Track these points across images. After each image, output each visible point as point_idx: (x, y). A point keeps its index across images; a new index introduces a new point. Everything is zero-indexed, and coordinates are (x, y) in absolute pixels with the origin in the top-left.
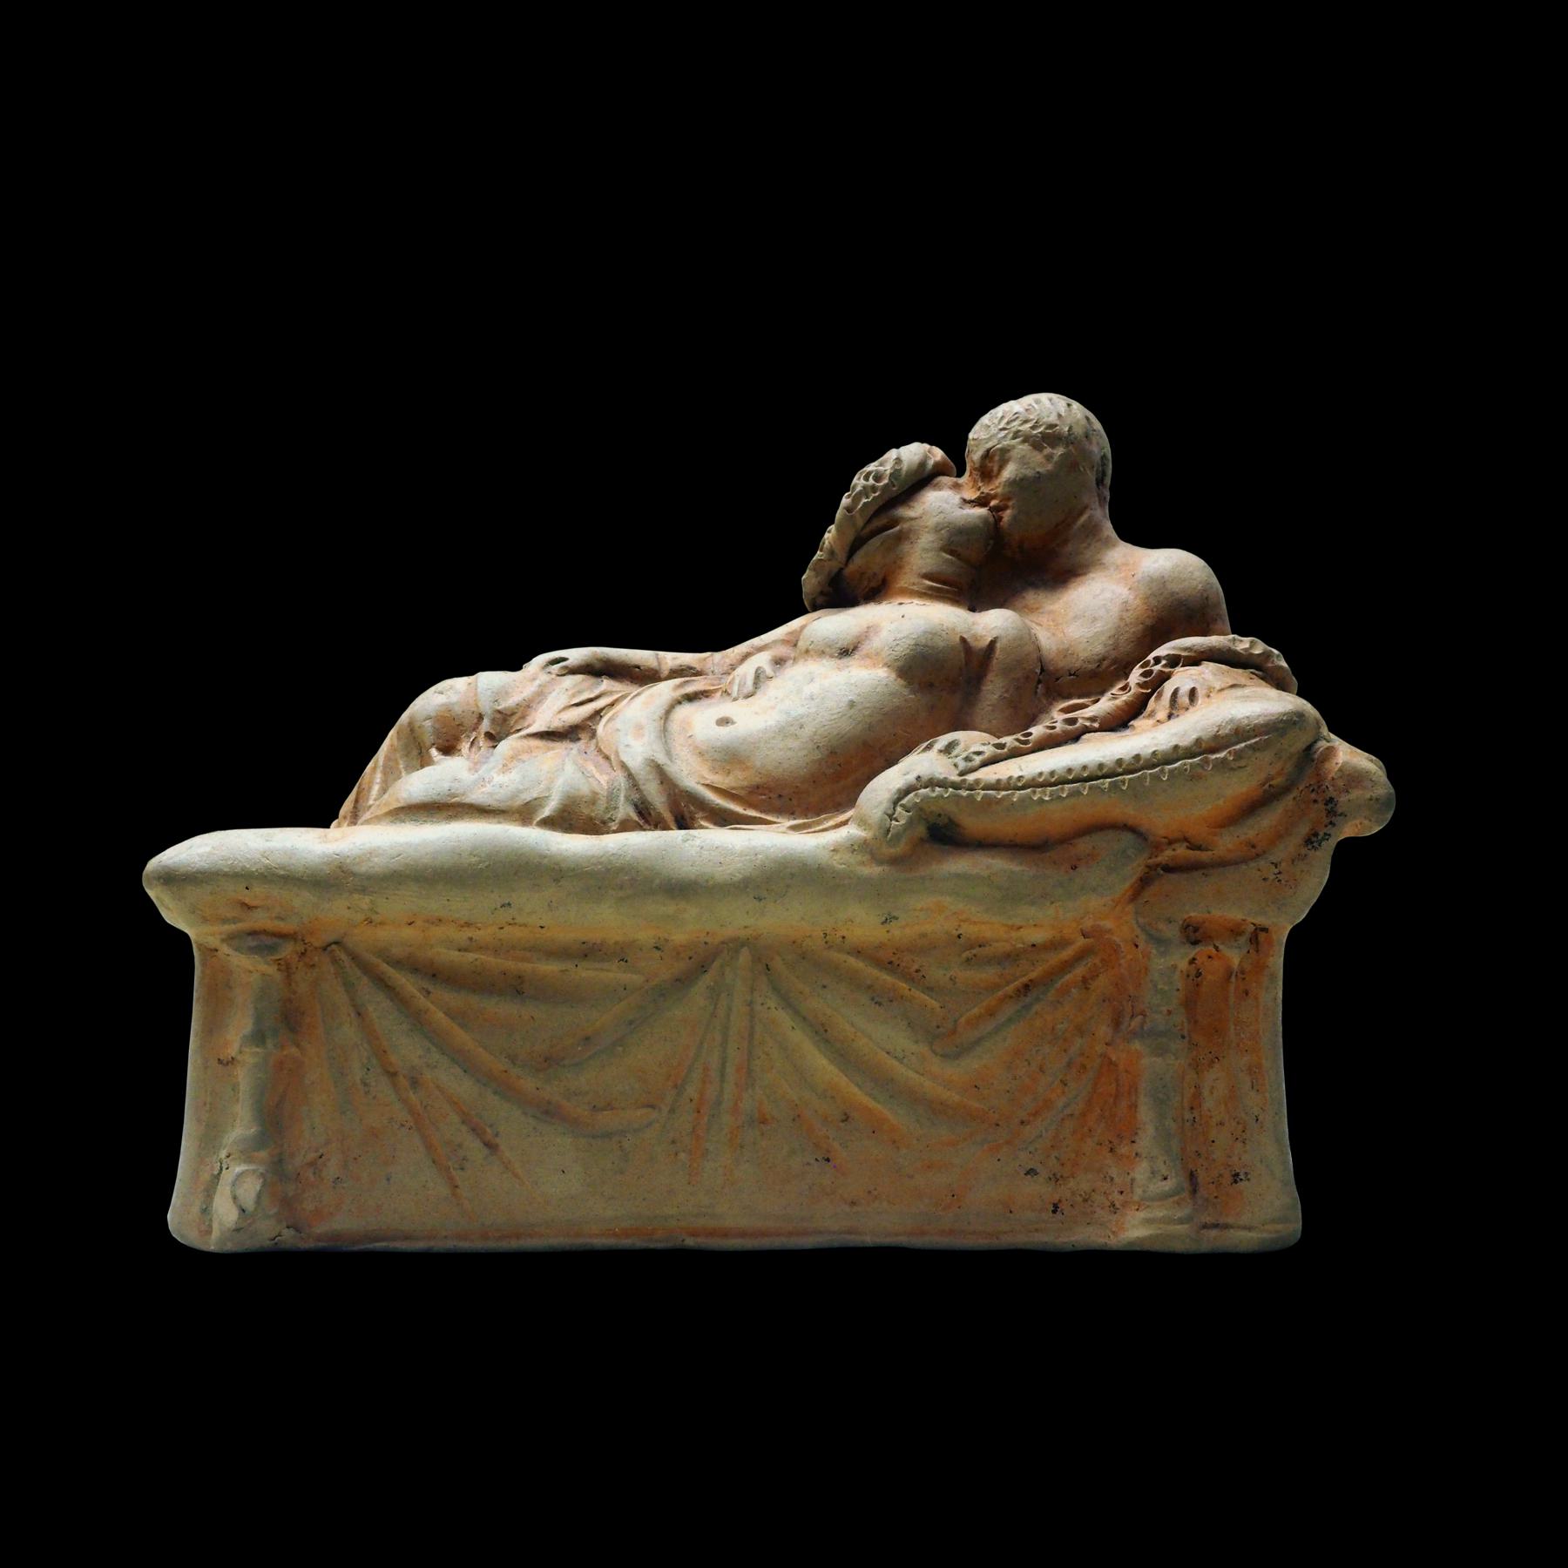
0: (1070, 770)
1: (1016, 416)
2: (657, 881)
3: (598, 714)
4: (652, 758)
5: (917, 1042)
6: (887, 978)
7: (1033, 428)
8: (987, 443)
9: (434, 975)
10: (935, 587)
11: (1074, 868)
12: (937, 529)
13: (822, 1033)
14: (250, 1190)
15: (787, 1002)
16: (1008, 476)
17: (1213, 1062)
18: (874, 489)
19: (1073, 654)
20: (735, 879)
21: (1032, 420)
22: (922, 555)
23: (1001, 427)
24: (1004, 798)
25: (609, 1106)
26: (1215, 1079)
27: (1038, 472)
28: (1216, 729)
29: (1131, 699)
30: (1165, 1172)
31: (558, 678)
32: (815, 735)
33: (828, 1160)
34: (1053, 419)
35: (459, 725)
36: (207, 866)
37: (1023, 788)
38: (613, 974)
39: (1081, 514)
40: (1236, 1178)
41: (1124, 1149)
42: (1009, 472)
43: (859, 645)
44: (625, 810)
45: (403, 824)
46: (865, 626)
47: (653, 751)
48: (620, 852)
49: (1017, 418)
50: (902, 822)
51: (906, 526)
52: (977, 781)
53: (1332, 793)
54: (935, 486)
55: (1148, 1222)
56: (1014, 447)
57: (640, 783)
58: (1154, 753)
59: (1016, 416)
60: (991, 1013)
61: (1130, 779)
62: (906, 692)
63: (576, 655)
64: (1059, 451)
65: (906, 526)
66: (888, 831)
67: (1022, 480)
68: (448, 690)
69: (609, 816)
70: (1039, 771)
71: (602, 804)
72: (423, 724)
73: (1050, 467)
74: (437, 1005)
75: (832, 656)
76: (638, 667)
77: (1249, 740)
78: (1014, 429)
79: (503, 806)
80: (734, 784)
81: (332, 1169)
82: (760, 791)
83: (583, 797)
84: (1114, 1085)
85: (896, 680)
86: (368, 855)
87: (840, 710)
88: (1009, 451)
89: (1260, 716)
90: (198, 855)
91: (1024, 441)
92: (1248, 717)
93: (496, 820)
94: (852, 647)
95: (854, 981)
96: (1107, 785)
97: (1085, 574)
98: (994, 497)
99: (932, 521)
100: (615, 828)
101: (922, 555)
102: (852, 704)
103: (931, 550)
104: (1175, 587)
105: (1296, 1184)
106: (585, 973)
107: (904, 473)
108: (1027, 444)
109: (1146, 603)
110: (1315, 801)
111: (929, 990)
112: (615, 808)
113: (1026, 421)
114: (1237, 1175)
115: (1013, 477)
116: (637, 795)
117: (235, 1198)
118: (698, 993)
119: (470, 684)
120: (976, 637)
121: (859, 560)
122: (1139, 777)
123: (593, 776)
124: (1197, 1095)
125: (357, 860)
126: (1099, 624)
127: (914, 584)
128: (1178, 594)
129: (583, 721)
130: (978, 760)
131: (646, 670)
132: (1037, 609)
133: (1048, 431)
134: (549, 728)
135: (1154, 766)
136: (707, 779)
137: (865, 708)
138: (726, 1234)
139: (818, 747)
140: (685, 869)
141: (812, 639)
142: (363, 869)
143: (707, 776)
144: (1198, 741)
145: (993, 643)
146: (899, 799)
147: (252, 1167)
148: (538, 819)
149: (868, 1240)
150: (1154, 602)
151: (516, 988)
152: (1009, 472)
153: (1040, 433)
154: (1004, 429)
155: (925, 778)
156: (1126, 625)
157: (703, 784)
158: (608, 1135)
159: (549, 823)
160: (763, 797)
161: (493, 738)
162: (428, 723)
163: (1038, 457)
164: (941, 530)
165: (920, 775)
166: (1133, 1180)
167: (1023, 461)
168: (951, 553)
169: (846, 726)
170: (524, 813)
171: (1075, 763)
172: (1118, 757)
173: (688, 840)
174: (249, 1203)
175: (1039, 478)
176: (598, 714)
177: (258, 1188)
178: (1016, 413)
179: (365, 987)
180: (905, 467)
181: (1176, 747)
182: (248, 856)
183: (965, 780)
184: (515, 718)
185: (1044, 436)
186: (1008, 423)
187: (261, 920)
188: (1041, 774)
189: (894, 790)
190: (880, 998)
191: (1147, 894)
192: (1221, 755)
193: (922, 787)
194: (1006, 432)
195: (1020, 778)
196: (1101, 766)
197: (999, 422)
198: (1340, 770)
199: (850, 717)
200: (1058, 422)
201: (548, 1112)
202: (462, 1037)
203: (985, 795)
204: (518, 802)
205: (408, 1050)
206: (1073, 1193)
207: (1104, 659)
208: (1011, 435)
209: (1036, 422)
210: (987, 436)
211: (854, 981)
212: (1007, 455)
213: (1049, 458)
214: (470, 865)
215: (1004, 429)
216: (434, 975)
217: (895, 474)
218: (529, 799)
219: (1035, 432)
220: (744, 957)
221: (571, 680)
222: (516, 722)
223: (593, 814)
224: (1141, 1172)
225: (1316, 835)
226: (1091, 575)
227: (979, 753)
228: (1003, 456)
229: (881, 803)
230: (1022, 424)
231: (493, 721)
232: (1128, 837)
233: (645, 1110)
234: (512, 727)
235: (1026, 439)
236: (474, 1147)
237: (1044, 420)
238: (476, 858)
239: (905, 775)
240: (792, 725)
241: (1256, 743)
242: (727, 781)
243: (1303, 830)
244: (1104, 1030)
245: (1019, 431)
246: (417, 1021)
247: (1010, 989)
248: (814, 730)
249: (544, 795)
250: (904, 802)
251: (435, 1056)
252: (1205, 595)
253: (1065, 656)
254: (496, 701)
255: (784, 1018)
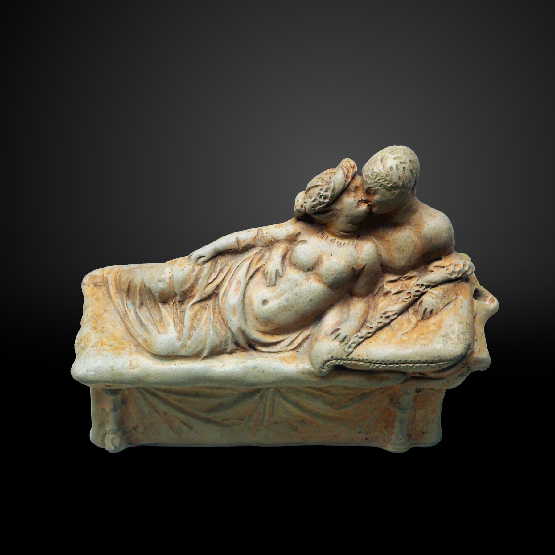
0: (383, 361)
1: (382, 177)
2: (244, 384)
3: (218, 287)
4: (240, 327)
5: (327, 406)
6: (319, 393)
7: (388, 184)
8: (369, 185)
9: (170, 392)
10: (346, 235)
11: (382, 380)
12: (347, 216)
13: (296, 405)
14: (117, 442)
15: (285, 398)
16: (376, 199)
17: (421, 409)
18: (323, 203)
19: (394, 263)
20: (270, 382)
21: (388, 180)
22: (341, 223)
23: (375, 181)
24: (360, 365)
25: (228, 419)
26: (420, 414)
27: (388, 199)
28: (433, 358)
29: (410, 302)
30: (401, 438)
31: (202, 266)
32: (297, 310)
33: (297, 430)
34: (396, 180)
35: (168, 296)
36: (94, 379)
37: (367, 362)
38: (228, 392)
39: (404, 205)
40: (423, 433)
41: (390, 429)
42: (376, 198)
43: (314, 267)
44: (231, 346)
45: (157, 359)
46: (317, 257)
47: (240, 324)
48: (232, 375)
49: (383, 178)
50: (326, 370)
51: (335, 212)
52: (352, 358)
53: (469, 365)
54: (348, 191)
55: (394, 448)
56: (380, 190)
57: (237, 337)
58: (412, 360)
59: (382, 177)
60: (352, 399)
61: (403, 366)
62: (330, 292)
63: (207, 250)
64: (398, 191)
65: (335, 212)
66: (321, 372)
67: (381, 202)
68: (163, 281)
69: (226, 348)
70: (373, 359)
71: (223, 344)
72: (155, 294)
73: (393, 197)
74: (172, 398)
75: (304, 271)
76: (231, 249)
77: (443, 362)
78: (381, 183)
79: (190, 355)
80: (268, 329)
81: (141, 430)
82: (277, 330)
83: (217, 345)
84: (388, 414)
85: (327, 289)
86: (148, 376)
87: (306, 302)
88: (378, 191)
89: (448, 356)
90: (91, 375)
91: (383, 188)
92: (444, 356)
93: (188, 359)
94: (312, 268)
95: (307, 393)
96: (395, 367)
97: (402, 226)
98: (371, 202)
99: (345, 213)
100: (228, 352)
101: (341, 223)
102: (311, 300)
103: (344, 223)
104: (434, 242)
105: (442, 426)
106: (219, 391)
107: (336, 194)
108: (385, 189)
109: (423, 246)
110: (464, 367)
111: (332, 394)
112: (228, 345)
113: (386, 181)
114: (424, 433)
115: (378, 200)
116: (235, 339)
117: (113, 444)
118: (257, 397)
119: (171, 278)
120: (358, 266)
121: (316, 217)
122: (406, 366)
123: (220, 332)
124: (415, 416)
125: (144, 377)
126: (404, 253)
127: (337, 232)
128: (436, 244)
129: (213, 292)
130: (354, 345)
131: (233, 250)
132: (383, 238)
133: (394, 185)
134: (201, 298)
135: (411, 363)
136: (259, 329)
137: (316, 301)
138: (264, 444)
139: (298, 314)
140: (253, 380)
141: (297, 261)
142: (147, 380)
143: (259, 327)
144: (427, 360)
145: (364, 267)
146: (325, 363)
147: (116, 436)
148: (202, 357)
149: (308, 444)
150: (426, 246)
151: (197, 395)
152: (376, 198)
153: (391, 186)
154: (376, 182)
155: (334, 358)
156: (415, 254)
157: (258, 331)
158: (227, 426)
159: (206, 357)
160: (279, 331)
161: (181, 302)
162: (157, 294)
163: (389, 194)
164: (348, 217)
165: (333, 357)
166: (391, 438)
167: (383, 195)
168: (352, 224)
169: (308, 308)
170: (196, 355)
171: (385, 359)
172: (400, 360)
173: (254, 369)
174: (117, 444)
175: (388, 201)
176: (218, 287)
177: (120, 441)
178: (382, 176)
179: (148, 396)
180: (336, 192)
181: (419, 360)
182: (107, 376)
183: (348, 358)
184: (188, 293)
185: (392, 187)
186: (378, 180)
187: (112, 388)
188: (373, 360)
189: (324, 360)
190: (315, 397)
191: (405, 384)
192: (434, 365)
193: (333, 360)
194: (377, 183)
195: (366, 360)
196: (394, 361)
197: (375, 178)
198: (474, 360)
199: (310, 305)
200: (399, 182)
201: (208, 421)
202: (179, 404)
203: (354, 363)
204: (195, 352)
205: (163, 408)
206: (372, 436)
207: (405, 266)
208: (379, 185)
209: (390, 181)
210: (370, 182)
211: (307, 393)
212: (377, 192)
213: (393, 194)
214: (182, 381)
215: (376, 182)
216: (170, 392)
217: (332, 196)
218: (199, 350)
219: (389, 185)
220: (272, 390)
221: (208, 265)
222: (189, 294)
223: (221, 349)
224: (393, 437)
225: (462, 374)
226: (405, 227)
227: (353, 343)
228: (376, 192)
229: (319, 363)
230: (384, 182)
231: (181, 296)
232: (399, 376)
233: (238, 421)
234: (187, 296)
235: (385, 187)
236: (185, 428)
237: (393, 181)
238: (184, 380)
239: (328, 354)
240: (289, 306)
241: (446, 363)
242: (266, 329)
243: (459, 373)
244: (387, 401)
245: (383, 184)
246: (166, 402)
247: (358, 394)
248: (297, 308)
249: (204, 347)
250: (327, 364)
251: (171, 409)
252: (446, 243)
253: (391, 263)
254: (181, 287)
255: (284, 402)
